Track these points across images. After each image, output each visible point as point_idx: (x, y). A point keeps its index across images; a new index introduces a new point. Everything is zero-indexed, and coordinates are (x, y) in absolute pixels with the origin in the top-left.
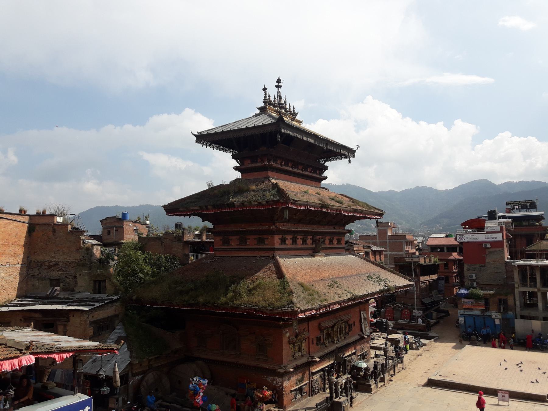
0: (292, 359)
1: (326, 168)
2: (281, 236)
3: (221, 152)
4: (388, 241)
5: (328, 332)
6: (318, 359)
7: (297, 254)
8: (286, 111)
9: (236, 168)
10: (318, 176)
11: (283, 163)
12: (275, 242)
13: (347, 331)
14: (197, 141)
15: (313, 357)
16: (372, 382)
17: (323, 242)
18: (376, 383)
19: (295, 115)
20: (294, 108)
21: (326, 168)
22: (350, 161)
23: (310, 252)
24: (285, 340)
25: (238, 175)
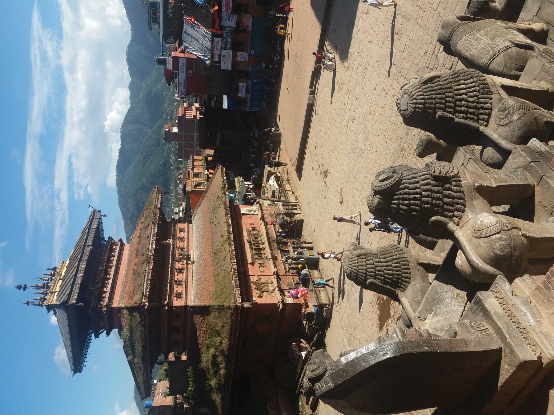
0: (273, 294)
1: (110, 238)
2: (175, 298)
3: (90, 345)
4: (184, 133)
5: (256, 254)
6: (276, 270)
7: (191, 280)
8: (52, 280)
9: (108, 334)
10: (118, 247)
11: (105, 289)
12: (179, 305)
13: (256, 232)
14: (81, 372)
15: (274, 274)
16: (297, 217)
17: (182, 249)
18: (297, 214)
19: (55, 269)
20: (48, 269)
21: (110, 238)
22: (104, 216)
23: (190, 266)
24: (260, 301)
25: (115, 331)
